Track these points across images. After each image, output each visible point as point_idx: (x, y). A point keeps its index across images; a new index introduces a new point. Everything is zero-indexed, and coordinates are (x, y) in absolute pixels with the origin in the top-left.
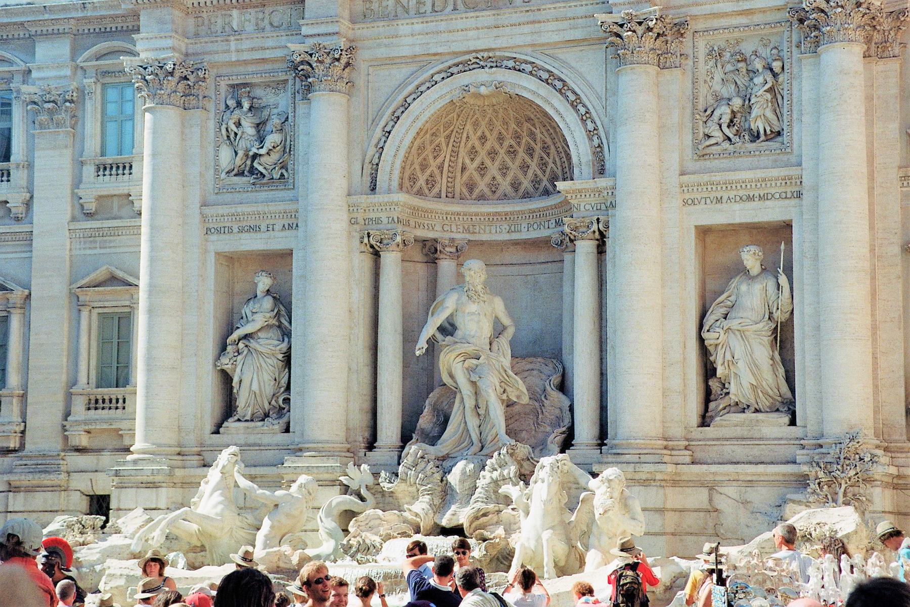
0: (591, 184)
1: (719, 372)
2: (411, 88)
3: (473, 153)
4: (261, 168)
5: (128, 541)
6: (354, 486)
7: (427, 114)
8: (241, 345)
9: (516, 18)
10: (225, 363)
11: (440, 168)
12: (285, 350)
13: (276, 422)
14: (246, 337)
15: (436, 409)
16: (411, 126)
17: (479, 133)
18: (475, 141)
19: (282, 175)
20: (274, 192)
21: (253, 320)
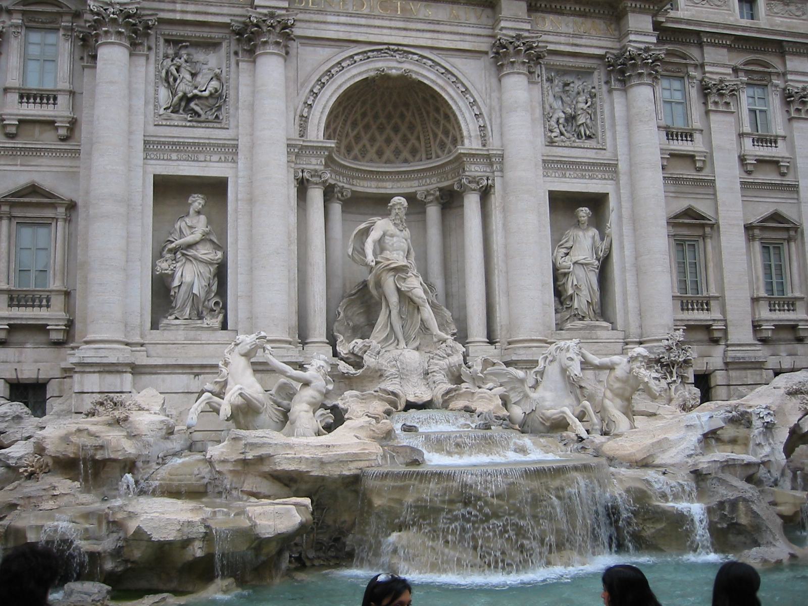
1: (570, 292)
2: (334, 63)
3: (354, 124)
4: (197, 109)
5: (162, 417)
8: (179, 255)
9: (420, 26)
10: (163, 266)
11: (335, 130)
12: (219, 261)
13: (214, 320)
15: (346, 316)
16: (335, 91)
17: (363, 110)
18: (358, 116)
19: (217, 117)
20: (210, 130)
21: (192, 233)
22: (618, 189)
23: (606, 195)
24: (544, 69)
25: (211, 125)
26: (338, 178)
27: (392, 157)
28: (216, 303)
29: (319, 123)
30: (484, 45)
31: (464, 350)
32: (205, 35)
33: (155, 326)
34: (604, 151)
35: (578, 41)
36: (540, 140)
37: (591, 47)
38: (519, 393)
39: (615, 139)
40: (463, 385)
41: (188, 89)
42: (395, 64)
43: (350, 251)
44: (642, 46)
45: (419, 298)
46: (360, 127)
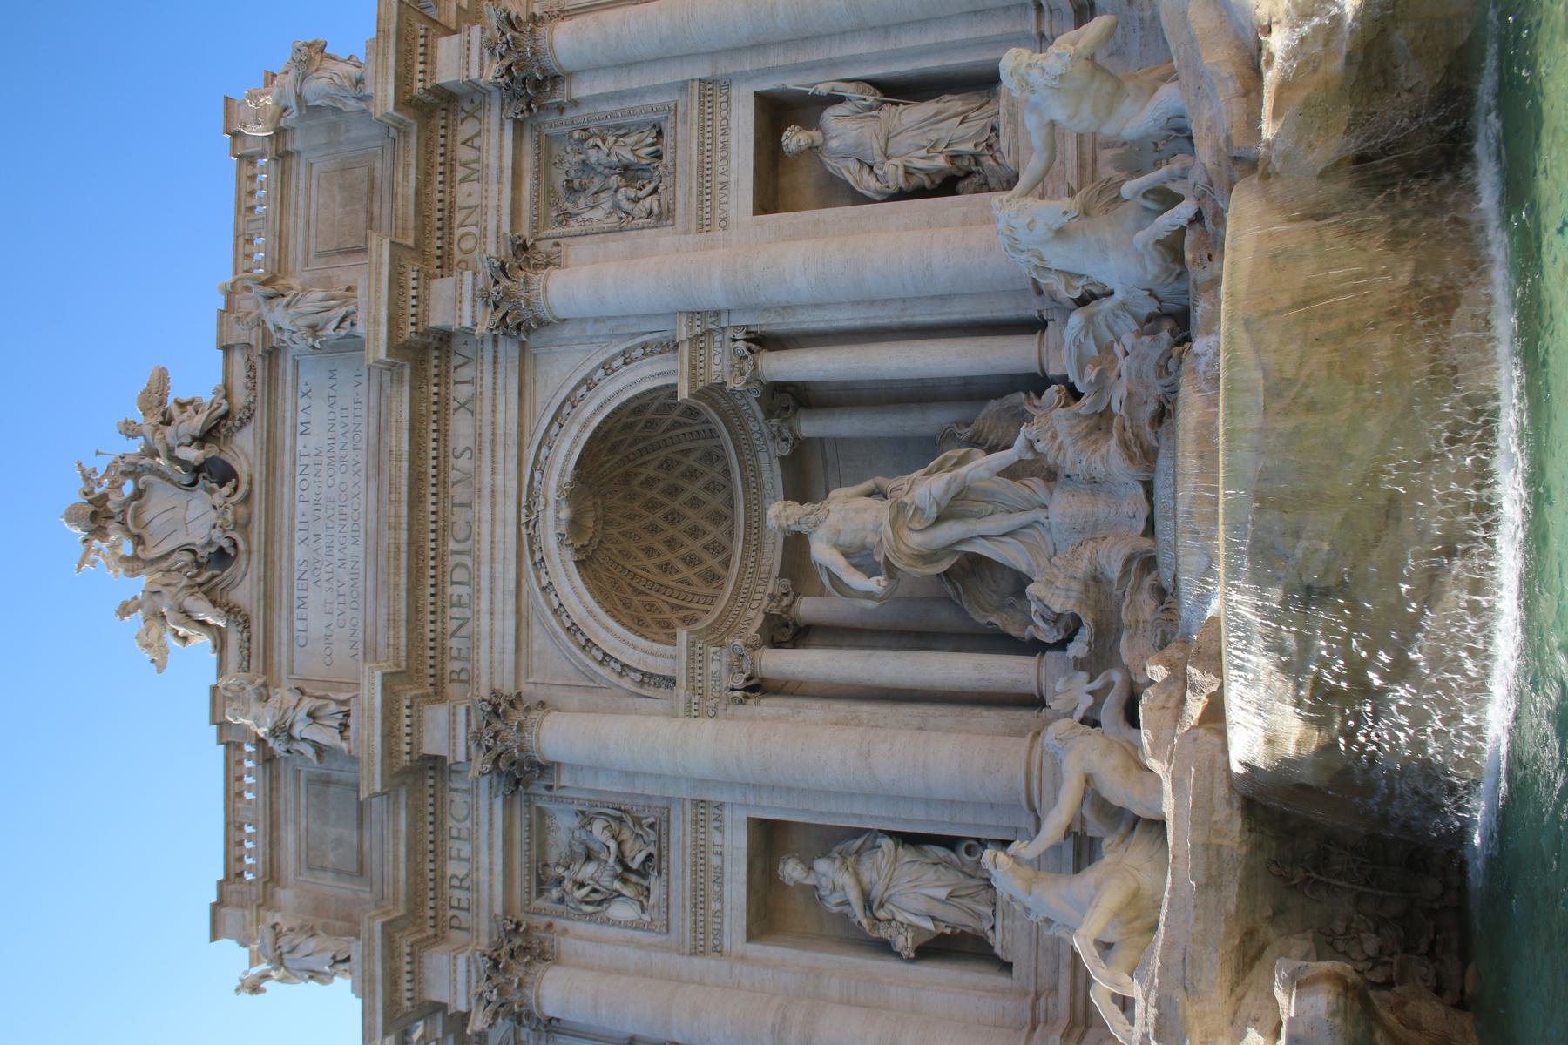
0: (685, 350)
1: (940, 162)
3: (666, 568)
4: (640, 858)
6: (1090, 700)
7: (588, 598)
8: (882, 914)
10: (904, 942)
12: (891, 843)
14: (868, 903)
15: (999, 608)
16: (599, 622)
17: (641, 555)
18: (651, 563)
20: (672, 840)
21: (843, 888)
22: (747, 77)
23: (759, 97)
24: (543, 234)
25: (664, 840)
26: (755, 604)
27: (721, 497)
28: (969, 851)
29: (652, 654)
30: (509, 350)
31: (1054, 387)
32: (526, 835)
33: (1007, 967)
34: (680, 108)
35: (494, 173)
36: (663, 238)
37: (501, 147)
38: (1117, 316)
39: (656, 90)
40: (1115, 406)
41: (608, 872)
42: (550, 513)
43: (871, 604)
44: (487, 52)
45: (949, 483)
46: (669, 556)
